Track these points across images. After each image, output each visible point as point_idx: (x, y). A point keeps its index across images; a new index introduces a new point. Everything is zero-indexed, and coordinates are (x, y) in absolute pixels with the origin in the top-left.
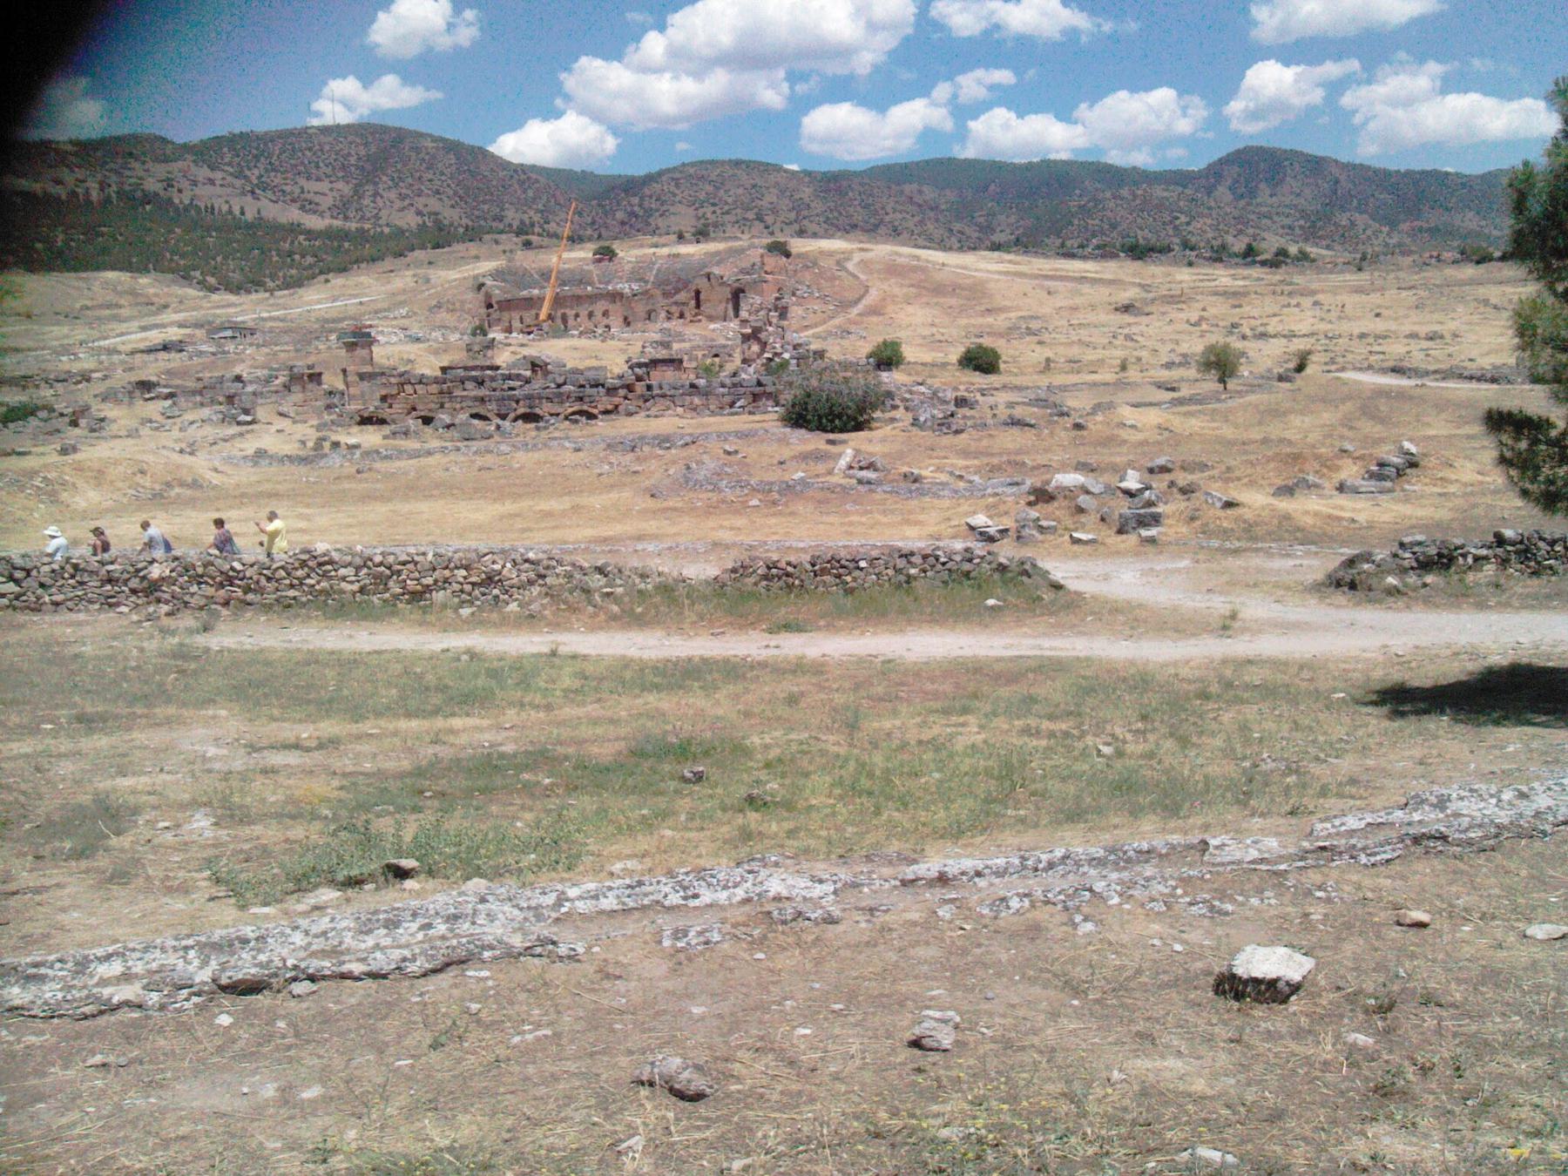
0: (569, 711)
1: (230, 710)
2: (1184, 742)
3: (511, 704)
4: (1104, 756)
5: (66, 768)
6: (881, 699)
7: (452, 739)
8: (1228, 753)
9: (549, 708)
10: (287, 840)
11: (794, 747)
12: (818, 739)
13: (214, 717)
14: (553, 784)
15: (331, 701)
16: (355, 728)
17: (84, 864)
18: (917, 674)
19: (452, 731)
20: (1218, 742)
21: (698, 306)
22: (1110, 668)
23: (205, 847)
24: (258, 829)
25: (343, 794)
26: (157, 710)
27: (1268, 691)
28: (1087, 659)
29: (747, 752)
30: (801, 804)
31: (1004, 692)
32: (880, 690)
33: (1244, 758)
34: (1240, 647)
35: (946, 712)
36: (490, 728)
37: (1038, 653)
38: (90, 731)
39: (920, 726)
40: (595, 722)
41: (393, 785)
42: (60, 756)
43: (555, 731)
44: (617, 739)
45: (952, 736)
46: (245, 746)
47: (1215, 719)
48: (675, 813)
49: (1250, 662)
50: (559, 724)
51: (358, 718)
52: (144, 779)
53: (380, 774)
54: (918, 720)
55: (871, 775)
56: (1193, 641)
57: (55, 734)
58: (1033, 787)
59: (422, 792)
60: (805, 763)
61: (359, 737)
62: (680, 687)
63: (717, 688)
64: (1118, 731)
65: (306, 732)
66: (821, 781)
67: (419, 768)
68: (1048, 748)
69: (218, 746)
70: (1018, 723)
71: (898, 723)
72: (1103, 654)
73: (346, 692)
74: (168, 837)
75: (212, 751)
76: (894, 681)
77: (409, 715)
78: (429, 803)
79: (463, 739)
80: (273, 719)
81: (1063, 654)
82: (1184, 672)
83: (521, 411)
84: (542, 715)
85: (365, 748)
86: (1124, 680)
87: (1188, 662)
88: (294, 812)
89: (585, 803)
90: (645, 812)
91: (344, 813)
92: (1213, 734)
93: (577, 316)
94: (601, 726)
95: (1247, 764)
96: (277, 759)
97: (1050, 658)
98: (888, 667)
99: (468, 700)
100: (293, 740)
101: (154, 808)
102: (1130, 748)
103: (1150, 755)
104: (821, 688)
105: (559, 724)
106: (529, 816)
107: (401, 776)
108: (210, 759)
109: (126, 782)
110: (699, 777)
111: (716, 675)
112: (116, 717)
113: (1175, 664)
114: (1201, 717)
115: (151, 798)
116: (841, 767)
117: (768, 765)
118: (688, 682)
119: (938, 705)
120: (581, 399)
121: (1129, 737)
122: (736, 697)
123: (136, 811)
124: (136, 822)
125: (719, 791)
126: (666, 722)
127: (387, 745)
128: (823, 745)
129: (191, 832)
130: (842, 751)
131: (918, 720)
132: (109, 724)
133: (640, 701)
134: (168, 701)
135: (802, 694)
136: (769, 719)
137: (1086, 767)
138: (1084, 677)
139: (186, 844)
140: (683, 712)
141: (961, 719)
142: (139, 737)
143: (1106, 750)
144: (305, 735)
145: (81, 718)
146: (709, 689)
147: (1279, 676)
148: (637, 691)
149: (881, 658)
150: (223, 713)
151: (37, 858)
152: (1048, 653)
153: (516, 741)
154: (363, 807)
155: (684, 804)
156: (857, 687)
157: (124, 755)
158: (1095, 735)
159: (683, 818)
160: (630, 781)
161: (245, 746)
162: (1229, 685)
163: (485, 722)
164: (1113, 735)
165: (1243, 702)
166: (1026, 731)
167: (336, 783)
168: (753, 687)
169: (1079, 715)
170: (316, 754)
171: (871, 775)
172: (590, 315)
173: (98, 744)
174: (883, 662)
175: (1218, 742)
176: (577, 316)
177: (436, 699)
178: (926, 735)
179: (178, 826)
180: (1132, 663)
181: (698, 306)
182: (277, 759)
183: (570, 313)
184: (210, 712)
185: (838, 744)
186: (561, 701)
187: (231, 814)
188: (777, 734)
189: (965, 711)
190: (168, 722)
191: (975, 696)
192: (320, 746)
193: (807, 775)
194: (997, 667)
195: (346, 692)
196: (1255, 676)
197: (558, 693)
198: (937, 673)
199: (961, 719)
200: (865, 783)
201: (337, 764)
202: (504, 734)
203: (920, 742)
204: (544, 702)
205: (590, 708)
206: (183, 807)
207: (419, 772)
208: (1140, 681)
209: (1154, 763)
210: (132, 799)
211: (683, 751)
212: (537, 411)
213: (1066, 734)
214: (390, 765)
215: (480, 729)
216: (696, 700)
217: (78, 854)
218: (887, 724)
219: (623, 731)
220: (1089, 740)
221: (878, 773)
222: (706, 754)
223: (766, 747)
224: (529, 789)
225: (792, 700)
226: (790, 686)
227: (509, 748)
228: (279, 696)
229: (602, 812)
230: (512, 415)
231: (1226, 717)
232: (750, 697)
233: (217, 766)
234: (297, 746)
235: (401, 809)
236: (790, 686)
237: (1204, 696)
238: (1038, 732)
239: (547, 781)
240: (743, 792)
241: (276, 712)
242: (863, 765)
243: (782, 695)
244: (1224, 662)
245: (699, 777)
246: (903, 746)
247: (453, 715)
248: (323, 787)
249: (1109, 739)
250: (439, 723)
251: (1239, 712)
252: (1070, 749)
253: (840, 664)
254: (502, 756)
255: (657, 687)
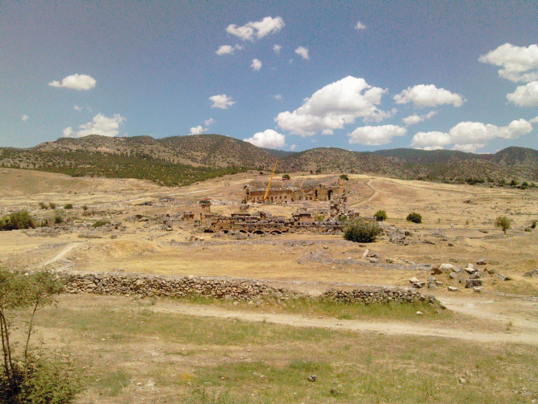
0: (269, 346)
1: (160, 337)
2: (492, 379)
3: (250, 342)
4: (462, 383)
5: (108, 356)
6: (379, 350)
7: (230, 354)
8: (510, 386)
9: (262, 344)
10: (178, 394)
11: (348, 369)
12: (356, 366)
13: (155, 340)
14: (264, 378)
15: (192, 336)
16: (199, 347)
17: (115, 398)
18: (392, 340)
19: (231, 352)
20: (506, 380)
21: (316, 196)
22: (464, 344)
23: (151, 394)
24: (168, 389)
25: (193, 375)
26: (137, 336)
27: (524, 358)
28: (455, 339)
29: (330, 369)
30: (350, 395)
31: (424, 351)
32: (378, 346)
33: (515, 389)
34: (513, 338)
35: (403, 358)
36: (243, 351)
37: (437, 335)
38: (117, 342)
39: (393, 363)
40: (278, 351)
41: (211, 373)
42: (107, 351)
43: (265, 354)
44: (286, 359)
45: (405, 369)
46: (165, 352)
47: (504, 369)
48: (306, 395)
49: (517, 345)
50: (267, 351)
51: (200, 344)
52: (133, 364)
53: (206, 368)
54: (392, 360)
55: (375, 384)
56: (495, 334)
57: (105, 342)
58: (436, 395)
59: (220, 377)
60: (352, 377)
61: (201, 351)
62: (307, 339)
63: (320, 340)
64: (468, 372)
65: (184, 348)
66: (357, 385)
67: (219, 367)
68: (441, 378)
69: (156, 351)
70: (430, 365)
71: (385, 361)
72: (461, 337)
73: (196, 332)
74: (140, 389)
75: (154, 354)
76: (382, 343)
77: (217, 344)
78: (223, 382)
79: (234, 355)
80: (173, 341)
81: (447, 336)
82: (492, 347)
83: (256, 230)
84: (260, 347)
85: (202, 356)
86: (470, 349)
87: (493, 343)
88: (179, 382)
89: (274, 388)
90: (295, 393)
91: (195, 384)
92: (503, 376)
93: (276, 198)
94: (280, 354)
95: (516, 392)
96: (174, 358)
97: (441, 337)
98: (381, 337)
99: (235, 339)
100: (179, 351)
101: (136, 376)
102: (472, 380)
103: (479, 384)
104: (358, 344)
105: (267, 351)
106: (256, 391)
107: (214, 369)
108: (154, 357)
109: (128, 364)
110: (314, 379)
111: (320, 335)
112: (124, 337)
113: (488, 344)
114: (499, 367)
115: (135, 372)
116: (364, 379)
117: (338, 376)
118: (310, 337)
119: (398, 354)
120: (276, 227)
121: (472, 374)
122: (326, 345)
123: (130, 377)
124: (130, 381)
125: (321, 386)
126: (302, 354)
127: (209, 355)
128: (358, 369)
129: (147, 388)
130: (365, 372)
131: (392, 360)
132: (123, 339)
133: (293, 344)
134: (141, 332)
135: (350, 346)
136: (338, 355)
137: (455, 388)
138: (454, 347)
139: (146, 392)
140: (310, 350)
141: (408, 362)
142: (132, 346)
143: (463, 380)
144: (183, 349)
145: (113, 337)
146: (317, 341)
147: (529, 352)
148: (292, 340)
149: (378, 333)
150: (157, 338)
151: (101, 394)
152: (440, 335)
153: (251, 357)
154: (202, 382)
155: (309, 391)
156: (370, 344)
157: (127, 353)
158: (459, 373)
159: (308, 398)
160: (290, 379)
161: (165, 352)
162: (509, 354)
163: (241, 348)
164: (465, 374)
165: (515, 362)
166: (433, 369)
167: (193, 370)
168: (333, 341)
169: (453, 363)
170: (187, 357)
171: (375, 384)
172: (281, 198)
173: (119, 348)
174: (379, 334)
175: (506, 380)
177: (225, 338)
178: (395, 368)
179: (143, 385)
180: (472, 342)
181: (316, 196)
182: (174, 358)
183: (274, 197)
184: (154, 338)
185: (364, 369)
186: (266, 341)
187: (161, 382)
188: (342, 362)
189: (410, 358)
190: (141, 341)
191: (413, 352)
192: (188, 354)
193: (352, 382)
194: (423, 340)
195: (196, 332)
196: (520, 351)
197: (266, 338)
198: (399, 340)
199: (408, 362)
200: (373, 387)
201: (195, 362)
202: (248, 354)
203: (393, 370)
204: (261, 342)
205: (276, 345)
206: (145, 376)
207: (219, 368)
208: (475, 350)
209: (480, 388)
210: (129, 371)
211: (308, 368)
212: (262, 230)
213: (448, 372)
214: (210, 364)
215: (239, 351)
216: (312, 345)
217: (113, 394)
218: (381, 361)
219: (288, 356)
220: (457, 375)
221: (378, 383)
222: (316, 369)
223: (338, 368)
224: (255, 378)
225: (347, 348)
226: (347, 341)
227: (249, 360)
228: (175, 332)
229: (280, 392)
230: (253, 231)
231: (509, 369)
232: (331, 345)
233: (155, 360)
234: (180, 354)
235: (214, 384)
236: (347, 341)
237: (500, 359)
238: (437, 370)
239: (262, 376)
240: (330, 388)
241: (174, 339)
242: (373, 379)
243: (344, 345)
244: (508, 344)
245: (314, 379)
246: (387, 372)
247: (231, 344)
248: (189, 372)
249: (464, 375)
250: (226, 347)
251: (513, 367)
252: (449, 379)
253: (364, 334)
254: (247, 364)
255: (299, 338)
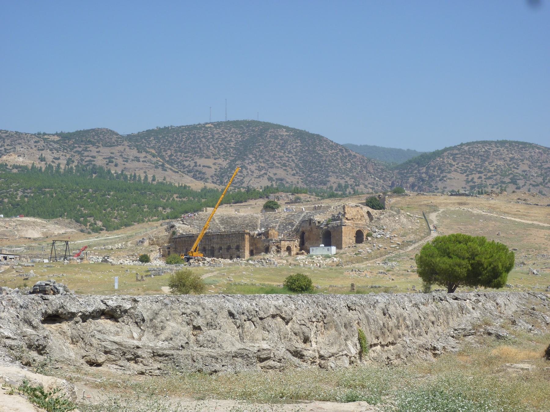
176: (221, 249)
